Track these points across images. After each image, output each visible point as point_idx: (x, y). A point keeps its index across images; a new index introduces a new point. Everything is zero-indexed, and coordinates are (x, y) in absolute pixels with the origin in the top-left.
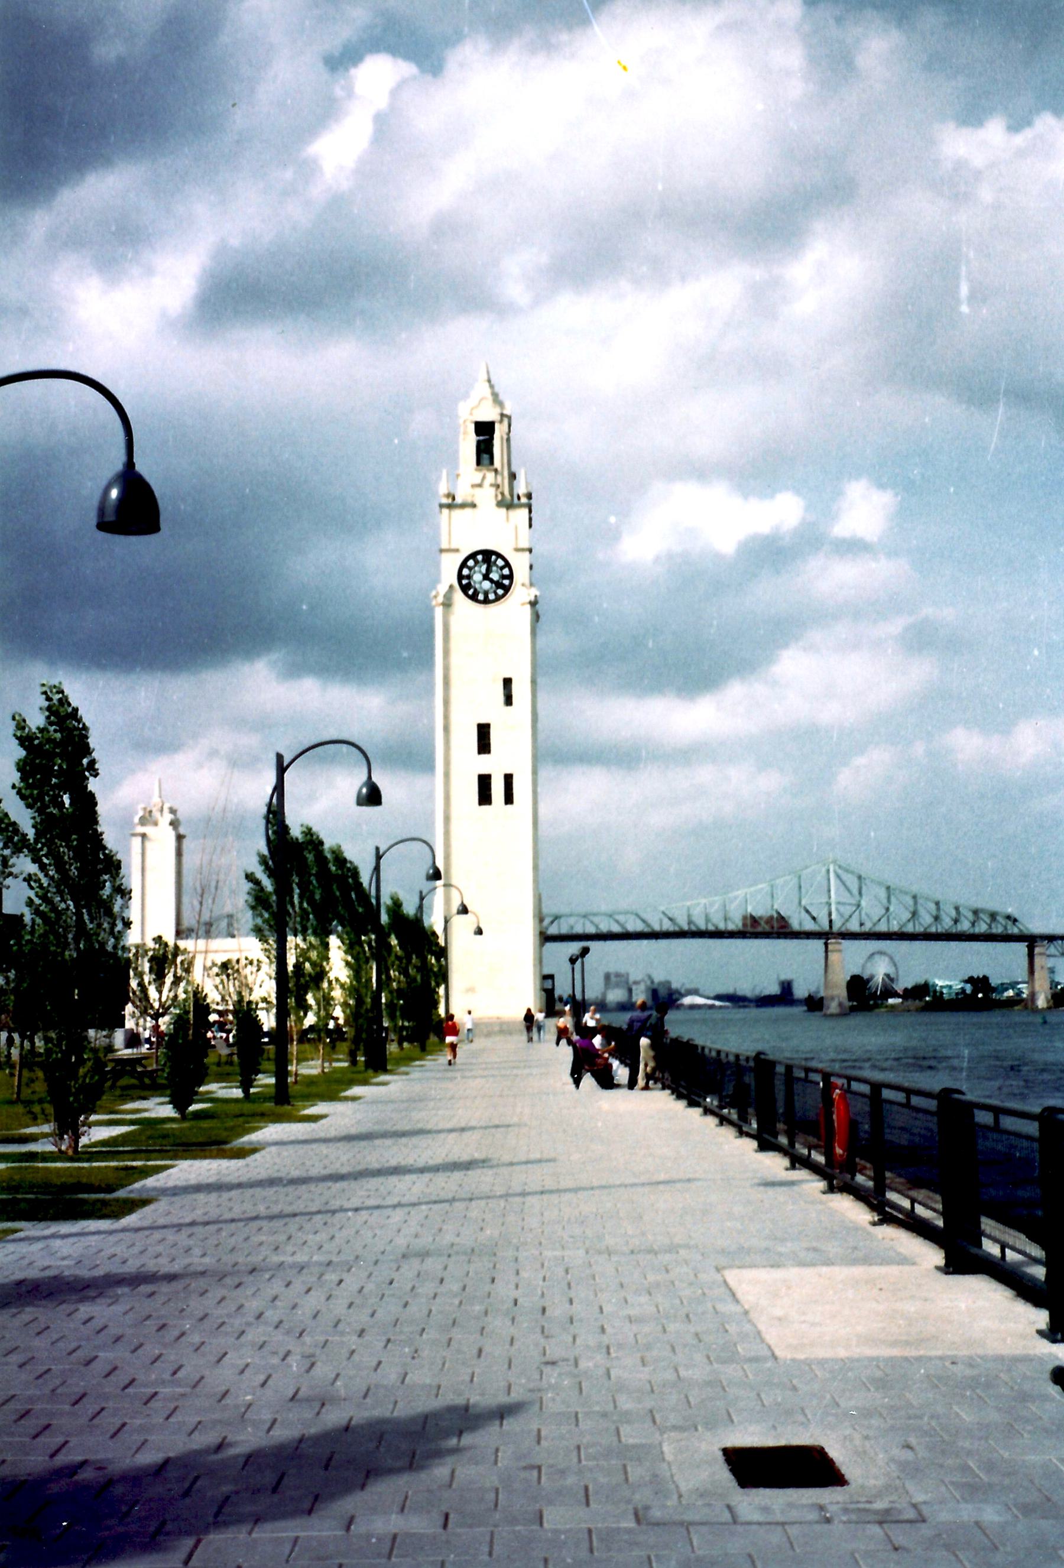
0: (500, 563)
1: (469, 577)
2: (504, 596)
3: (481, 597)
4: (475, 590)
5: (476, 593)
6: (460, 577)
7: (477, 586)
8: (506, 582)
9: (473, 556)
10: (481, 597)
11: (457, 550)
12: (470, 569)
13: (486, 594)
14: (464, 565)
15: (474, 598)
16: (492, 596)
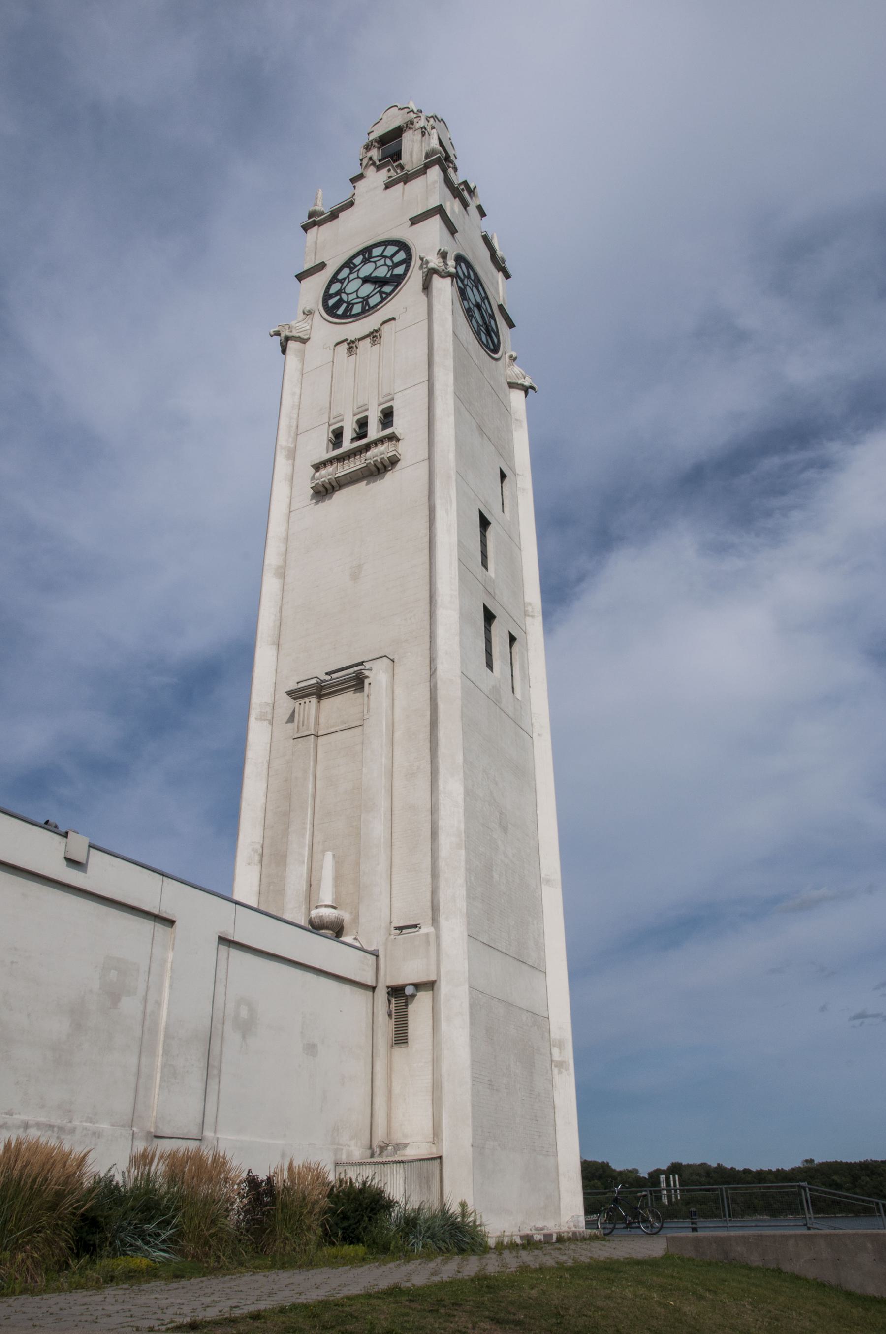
0: (391, 250)
4: (348, 303)
6: (327, 296)
9: (349, 264)
11: (322, 266)
12: (341, 281)
14: (334, 279)
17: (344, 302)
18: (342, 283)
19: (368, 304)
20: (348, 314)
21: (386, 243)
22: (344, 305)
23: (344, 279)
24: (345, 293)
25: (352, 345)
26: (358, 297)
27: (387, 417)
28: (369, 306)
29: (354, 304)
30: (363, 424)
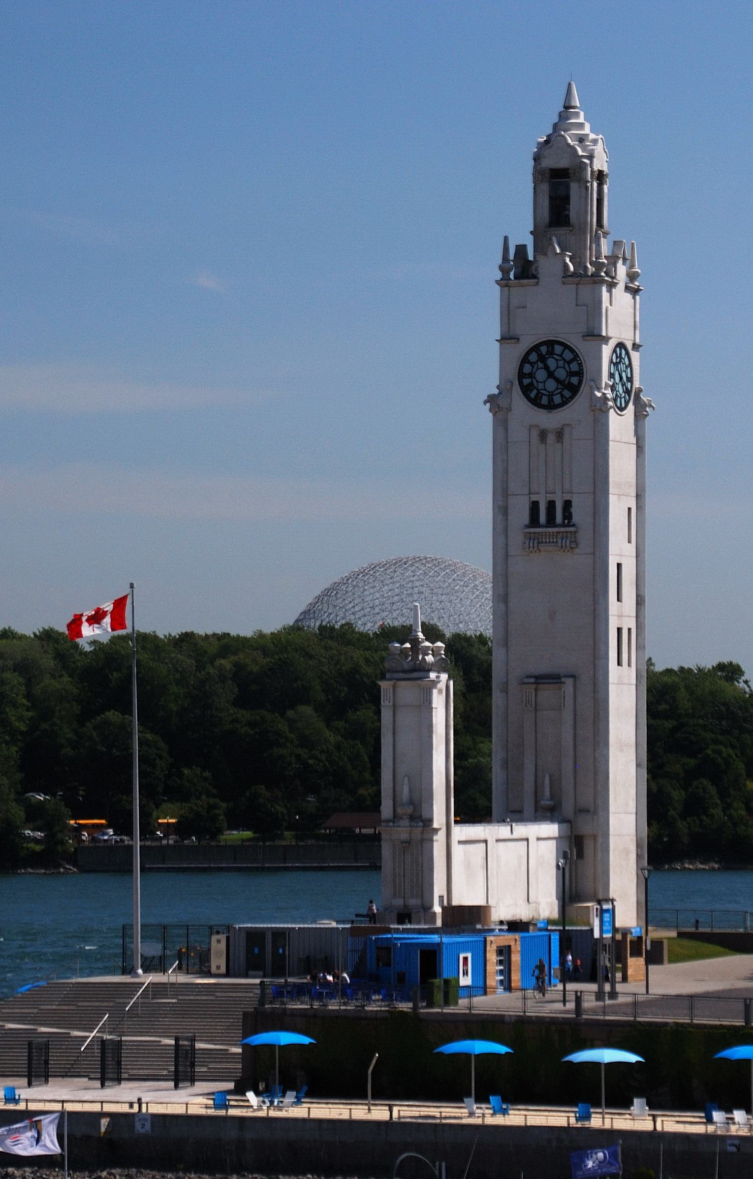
0: (568, 355)
1: (531, 375)
2: (572, 397)
3: (545, 401)
4: (538, 390)
5: (539, 395)
6: (521, 375)
7: (541, 386)
8: (574, 380)
9: (535, 348)
10: (545, 401)
13: (551, 395)
14: (525, 360)
15: (535, 402)
16: (557, 399)
17: (535, 388)
18: (533, 367)
19: (552, 400)
20: (539, 401)
21: (566, 347)
22: (535, 392)
23: (535, 363)
24: (535, 378)
25: (543, 435)
26: (545, 390)
27: (568, 504)
28: (554, 403)
29: (543, 394)
30: (551, 505)
